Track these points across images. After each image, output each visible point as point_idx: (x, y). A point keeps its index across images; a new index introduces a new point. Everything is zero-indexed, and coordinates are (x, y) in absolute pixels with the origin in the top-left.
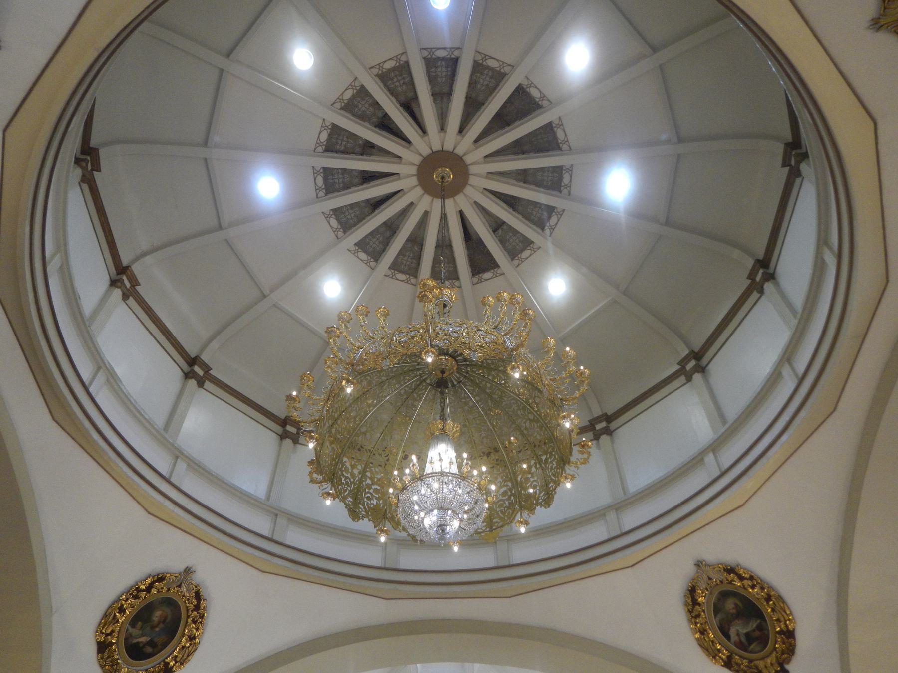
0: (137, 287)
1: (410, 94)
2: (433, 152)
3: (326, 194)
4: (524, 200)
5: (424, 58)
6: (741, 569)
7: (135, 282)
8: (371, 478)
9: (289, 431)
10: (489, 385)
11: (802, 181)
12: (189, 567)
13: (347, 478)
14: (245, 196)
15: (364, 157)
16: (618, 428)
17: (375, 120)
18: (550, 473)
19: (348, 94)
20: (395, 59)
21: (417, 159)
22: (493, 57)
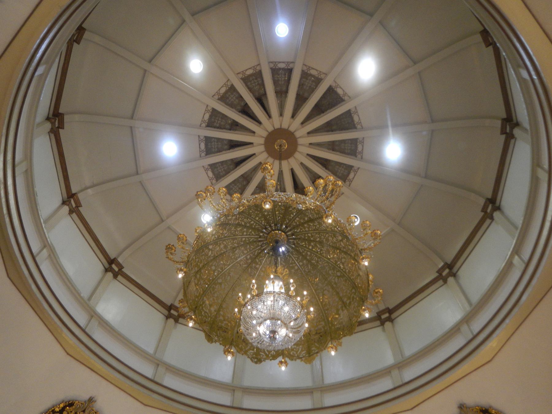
0: (80, 208)
1: (262, 92)
2: (275, 130)
3: (206, 155)
4: (333, 161)
5: (271, 68)
6: (493, 409)
7: (78, 205)
8: (223, 316)
9: (172, 314)
10: (309, 253)
11: (515, 142)
12: (93, 396)
13: (205, 312)
14: (155, 155)
15: (232, 131)
16: (398, 316)
17: (239, 108)
18: (353, 312)
19: (223, 90)
20: (253, 68)
21: (265, 134)
22: (314, 68)
